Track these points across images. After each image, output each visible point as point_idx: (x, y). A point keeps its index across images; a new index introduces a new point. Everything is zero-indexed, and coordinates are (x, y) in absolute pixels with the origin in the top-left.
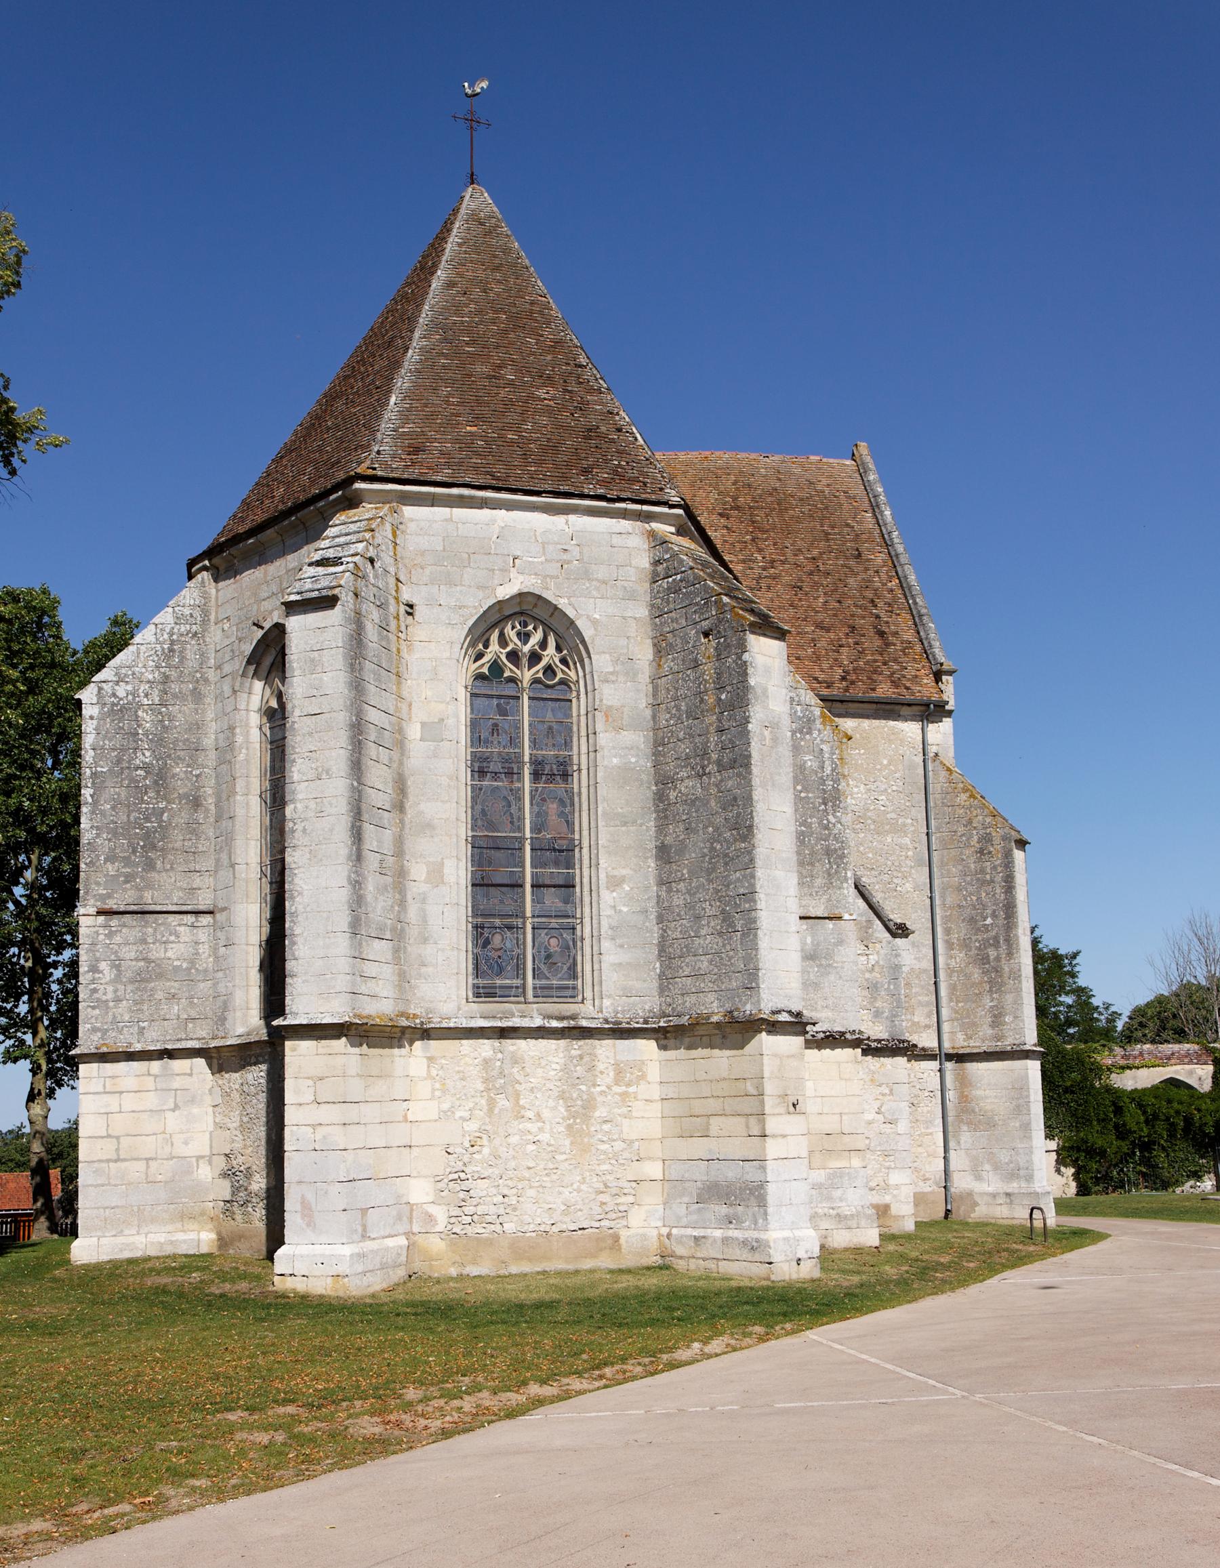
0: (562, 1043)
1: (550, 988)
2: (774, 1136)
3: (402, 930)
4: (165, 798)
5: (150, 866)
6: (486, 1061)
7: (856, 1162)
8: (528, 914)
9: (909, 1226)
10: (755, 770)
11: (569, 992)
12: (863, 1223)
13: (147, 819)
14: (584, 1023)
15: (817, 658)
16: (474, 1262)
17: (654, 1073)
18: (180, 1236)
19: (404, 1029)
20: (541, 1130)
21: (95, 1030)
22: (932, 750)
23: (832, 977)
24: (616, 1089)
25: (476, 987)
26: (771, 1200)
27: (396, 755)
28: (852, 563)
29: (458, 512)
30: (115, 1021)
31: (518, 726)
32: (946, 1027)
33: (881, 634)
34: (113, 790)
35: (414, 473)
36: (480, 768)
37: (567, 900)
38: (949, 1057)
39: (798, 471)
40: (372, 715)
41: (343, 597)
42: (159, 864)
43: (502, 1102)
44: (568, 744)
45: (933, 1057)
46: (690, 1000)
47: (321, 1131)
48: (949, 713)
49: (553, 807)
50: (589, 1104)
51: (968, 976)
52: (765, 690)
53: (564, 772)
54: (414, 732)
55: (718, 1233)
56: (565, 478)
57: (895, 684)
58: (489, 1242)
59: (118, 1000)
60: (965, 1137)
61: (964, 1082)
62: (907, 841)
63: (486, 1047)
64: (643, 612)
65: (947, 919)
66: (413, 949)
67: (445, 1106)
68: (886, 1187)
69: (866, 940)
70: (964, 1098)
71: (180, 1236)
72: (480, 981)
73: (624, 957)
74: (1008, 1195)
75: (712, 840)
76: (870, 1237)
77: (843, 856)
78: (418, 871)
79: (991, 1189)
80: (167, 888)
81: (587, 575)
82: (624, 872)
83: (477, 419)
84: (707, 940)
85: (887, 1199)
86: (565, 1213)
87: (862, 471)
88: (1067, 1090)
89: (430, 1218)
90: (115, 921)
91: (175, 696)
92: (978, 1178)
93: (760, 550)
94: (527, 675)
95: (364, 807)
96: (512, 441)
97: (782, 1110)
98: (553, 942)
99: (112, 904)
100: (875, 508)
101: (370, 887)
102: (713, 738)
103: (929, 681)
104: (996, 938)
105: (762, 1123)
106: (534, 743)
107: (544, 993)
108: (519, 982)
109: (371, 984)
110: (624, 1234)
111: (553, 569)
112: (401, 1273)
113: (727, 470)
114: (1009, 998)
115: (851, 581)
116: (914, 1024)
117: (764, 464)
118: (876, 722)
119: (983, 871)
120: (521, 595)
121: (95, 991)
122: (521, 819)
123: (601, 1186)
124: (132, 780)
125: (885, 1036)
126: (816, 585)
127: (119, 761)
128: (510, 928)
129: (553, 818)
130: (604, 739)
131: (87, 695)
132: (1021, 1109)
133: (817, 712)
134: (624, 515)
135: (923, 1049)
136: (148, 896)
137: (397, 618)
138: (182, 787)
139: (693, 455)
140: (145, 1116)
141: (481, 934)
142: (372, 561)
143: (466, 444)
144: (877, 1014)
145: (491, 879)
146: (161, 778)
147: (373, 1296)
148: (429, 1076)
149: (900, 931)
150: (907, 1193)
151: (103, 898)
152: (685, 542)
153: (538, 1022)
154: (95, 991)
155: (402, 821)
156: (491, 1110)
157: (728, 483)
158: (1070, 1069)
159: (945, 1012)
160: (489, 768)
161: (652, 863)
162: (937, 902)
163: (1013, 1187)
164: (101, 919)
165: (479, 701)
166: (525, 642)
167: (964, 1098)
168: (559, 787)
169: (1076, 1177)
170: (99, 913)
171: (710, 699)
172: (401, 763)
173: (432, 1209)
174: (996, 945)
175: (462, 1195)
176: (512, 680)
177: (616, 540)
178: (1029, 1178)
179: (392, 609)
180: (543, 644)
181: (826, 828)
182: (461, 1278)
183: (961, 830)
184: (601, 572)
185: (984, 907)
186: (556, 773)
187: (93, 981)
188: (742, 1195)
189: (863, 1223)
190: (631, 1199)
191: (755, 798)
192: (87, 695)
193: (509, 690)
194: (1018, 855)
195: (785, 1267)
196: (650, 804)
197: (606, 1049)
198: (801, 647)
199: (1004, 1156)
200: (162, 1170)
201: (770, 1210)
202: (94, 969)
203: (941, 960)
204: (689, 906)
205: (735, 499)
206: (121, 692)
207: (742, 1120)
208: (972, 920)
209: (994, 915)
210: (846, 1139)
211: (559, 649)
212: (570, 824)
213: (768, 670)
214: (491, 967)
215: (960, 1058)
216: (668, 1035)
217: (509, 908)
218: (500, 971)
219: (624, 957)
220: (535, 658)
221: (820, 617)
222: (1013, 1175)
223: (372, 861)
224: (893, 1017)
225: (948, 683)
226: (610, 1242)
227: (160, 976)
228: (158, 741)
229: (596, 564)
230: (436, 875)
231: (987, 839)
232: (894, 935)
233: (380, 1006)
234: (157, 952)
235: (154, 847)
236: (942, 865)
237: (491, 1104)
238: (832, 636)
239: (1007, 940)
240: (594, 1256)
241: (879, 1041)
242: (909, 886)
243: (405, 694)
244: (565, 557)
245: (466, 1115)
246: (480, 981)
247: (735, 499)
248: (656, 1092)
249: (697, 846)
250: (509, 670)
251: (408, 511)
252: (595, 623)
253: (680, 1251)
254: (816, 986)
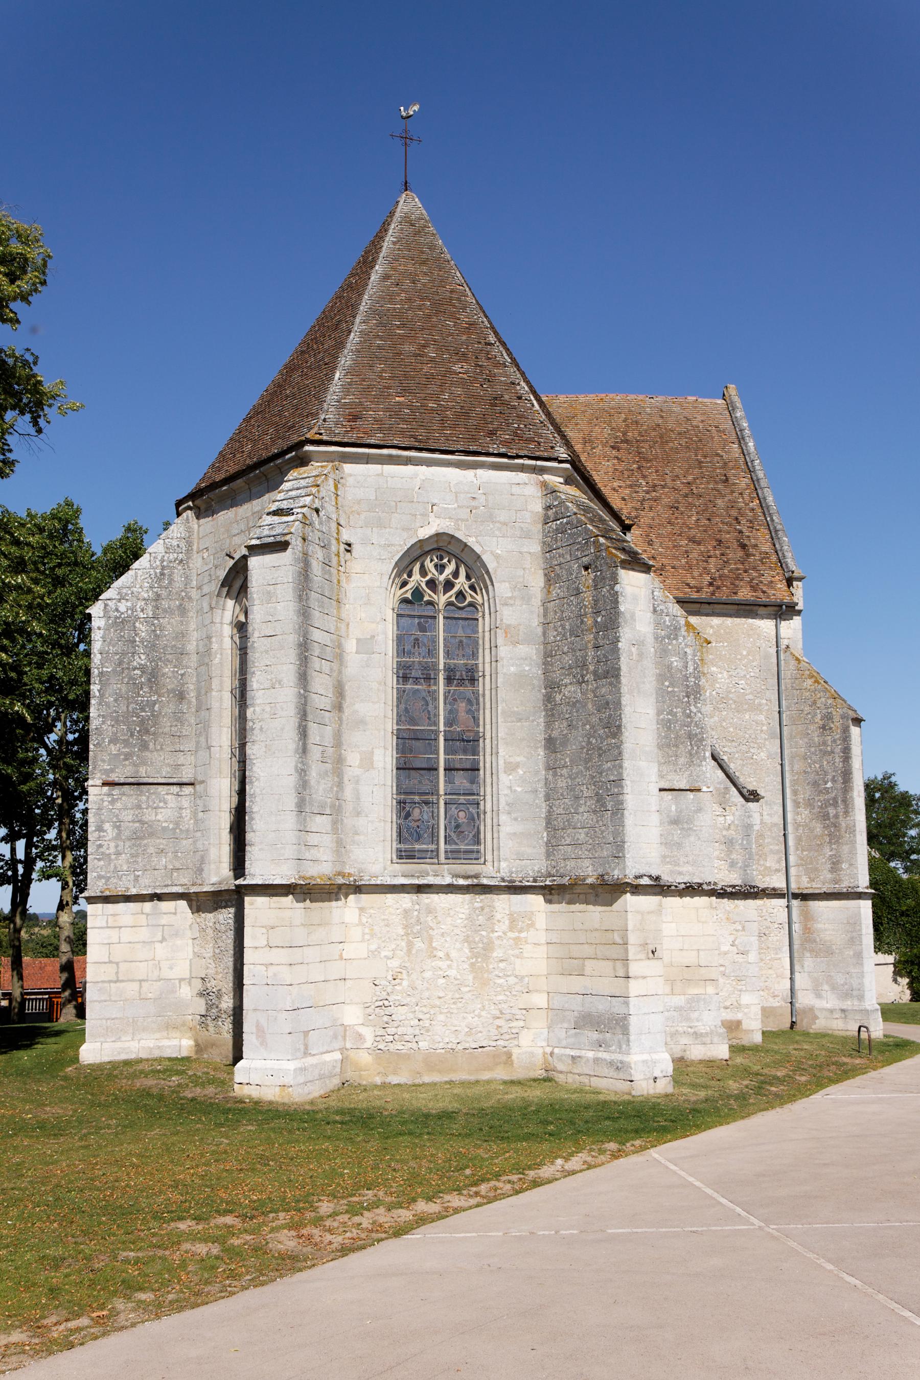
0: (467, 897)
1: (458, 851)
2: (636, 978)
3: (340, 806)
4: (156, 693)
5: (144, 747)
6: (406, 911)
7: (710, 990)
8: (442, 792)
9: (758, 1038)
10: (624, 680)
11: (473, 855)
12: (716, 1040)
13: (143, 710)
14: (485, 881)
15: (689, 567)
16: (395, 1073)
17: (541, 921)
18: (166, 1043)
19: (340, 887)
20: (449, 967)
21: (100, 877)
22: (784, 643)
23: (692, 839)
24: (510, 934)
25: (399, 850)
26: (632, 1029)
27: (335, 666)
28: (720, 486)
29: (387, 468)
30: (116, 870)
31: (434, 640)
32: (793, 871)
33: (743, 546)
34: (115, 686)
35: (352, 437)
36: (404, 674)
37: (473, 781)
38: (796, 896)
39: (677, 409)
40: (316, 635)
41: (293, 542)
42: (151, 746)
43: (419, 944)
44: (474, 655)
45: (782, 896)
46: (571, 864)
47: (272, 969)
48: (799, 613)
49: (462, 706)
50: (489, 947)
51: (812, 830)
52: (633, 616)
53: (472, 677)
54: (350, 646)
55: (590, 1054)
56: (474, 439)
57: (754, 588)
58: (407, 1057)
59: (118, 854)
60: (808, 963)
61: (807, 917)
62: (762, 718)
63: (406, 900)
64: (535, 547)
65: (794, 782)
66: (349, 821)
67: (373, 947)
68: (739, 1007)
69: (724, 804)
70: (807, 930)
71: (166, 1043)
72: (402, 846)
73: (518, 828)
74: (843, 1011)
75: (589, 736)
76: (722, 1051)
77: (702, 739)
78: (353, 758)
79: (829, 1006)
80: (157, 765)
81: (491, 518)
82: (518, 759)
83: (404, 391)
84: (584, 817)
85: (739, 1016)
86: (468, 1034)
87: (731, 408)
88: (902, 914)
89: (360, 1037)
90: (116, 791)
91: (165, 611)
92: (819, 996)
93: (644, 477)
94: (442, 599)
95: (308, 708)
96: (432, 409)
97: (643, 956)
98: (462, 814)
99: (114, 777)
100: (741, 440)
101: (313, 774)
102: (591, 653)
103: (782, 585)
104: (835, 799)
105: (627, 967)
106: (447, 654)
107: (453, 855)
108: (433, 847)
109: (314, 851)
110: (515, 1052)
111: (464, 513)
112: (336, 1081)
113: (619, 410)
114: (846, 849)
115: (719, 502)
116: (766, 868)
117: (649, 404)
118: (737, 620)
119: (825, 743)
120: (438, 535)
121: (100, 846)
122: (437, 715)
123: (497, 1013)
124: (131, 678)
125: (739, 882)
126: (690, 506)
127: (120, 663)
128: (427, 803)
129: (462, 715)
130: (504, 651)
131: (96, 610)
132: (854, 940)
133: (682, 621)
134: (522, 469)
135: (774, 889)
136: (142, 771)
137: (338, 555)
138: (170, 684)
139: (591, 397)
140: (139, 946)
141: (403, 808)
142: (317, 511)
143: (395, 412)
144: (733, 864)
145: (412, 764)
146: (153, 677)
147: (312, 1103)
148: (360, 923)
149: (752, 796)
150: (756, 1011)
151: (107, 772)
152: (572, 491)
153: (448, 880)
154: (100, 846)
155: (340, 719)
156: (409, 951)
157: (619, 421)
158: (906, 896)
159: (792, 859)
160: (411, 674)
161: (541, 752)
162: (787, 768)
163: (848, 1004)
164: (106, 789)
165: (403, 620)
166: (441, 571)
167: (807, 930)
168: (467, 689)
169: (910, 986)
170: (104, 784)
171: (589, 621)
172: (340, 672)
173: (364, 1030)
174: (835, 804)
175: (386, 1018)
176: (431, 603)
177: (516, 490)
178: (861, 998)
179: (334, 548)
180: (456, 574)
181: (689, 716)
182: (384, 1086)
183: (807, 709)
184: (502, 516)
185: (826, 773)
186: (465, 678)
187: (99, 838)
188: (611, 1025)
189: (716, 1040)
190: (521, 1023)
191: (623, 703)
192: (96, 610)
193: (428, 611)
194: (855, 731)
195: (644, 1084)
196: (540, 704)
197: (503, 903)
198: (676, 558)
199: (840, 979)
200: (152, 990)
201: (632, 1038)
202: (100, 829)
203: (790, 816)
204: (571, 789)
205: (624, 434)
206: (122, 608)
207: (610, 963)
208: (815, 784)
209: (834, 780)
210: (703, 970)
211: (468, 577)
212: (476, 720)
213: (635, 598)
214: (411, 835)
215: (804, 897)
216: (553, 892)
217: (426, 788)
218: (419, 838)
219: (518, 828)
220: (449, 585)
221: (693, 532)
222: (847, 995)
223: (315, 753)
224: (746, 867)
225: (798, 589)
226: (504, 1058)
227: (152, 835)
228: (152, 647)
229: (500, 510)
230: (368, 762)
231: (828, 717)
232: (747, 800)
233: (321, 868)
234: (149, 816)
235: (147, 732)
236: (791, 737)
237: (410, 945)
238: (702, 548)
239: (845, 801)
240: (490, 1069)
241: (734, 887)
242: (763, 755)
243: (343, 616)
244: (474, 503)
245: (390, 954)
246: (402, 846)
247: (624, 434)
248: (542, 937)
249: (577, 739)
250: (428, 595)
251: (348, 468)
252: (497, 557)
253: (560, 1067)
254: (679, 845)
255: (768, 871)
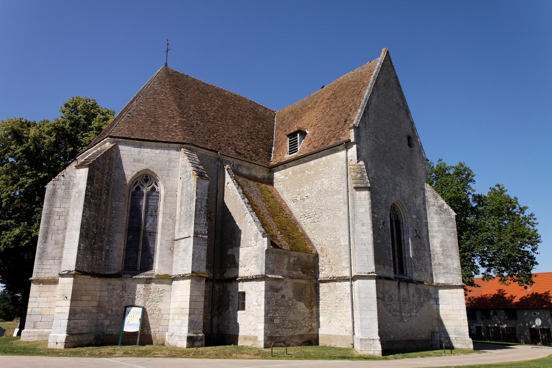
45: (348, 280)
97: (62, 299)
118: (332, 155)
125: (259, 274)
142: (63, 176)
255: (344, 268)
